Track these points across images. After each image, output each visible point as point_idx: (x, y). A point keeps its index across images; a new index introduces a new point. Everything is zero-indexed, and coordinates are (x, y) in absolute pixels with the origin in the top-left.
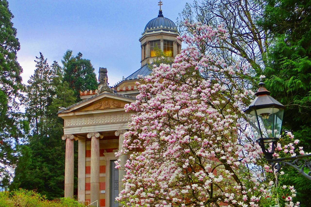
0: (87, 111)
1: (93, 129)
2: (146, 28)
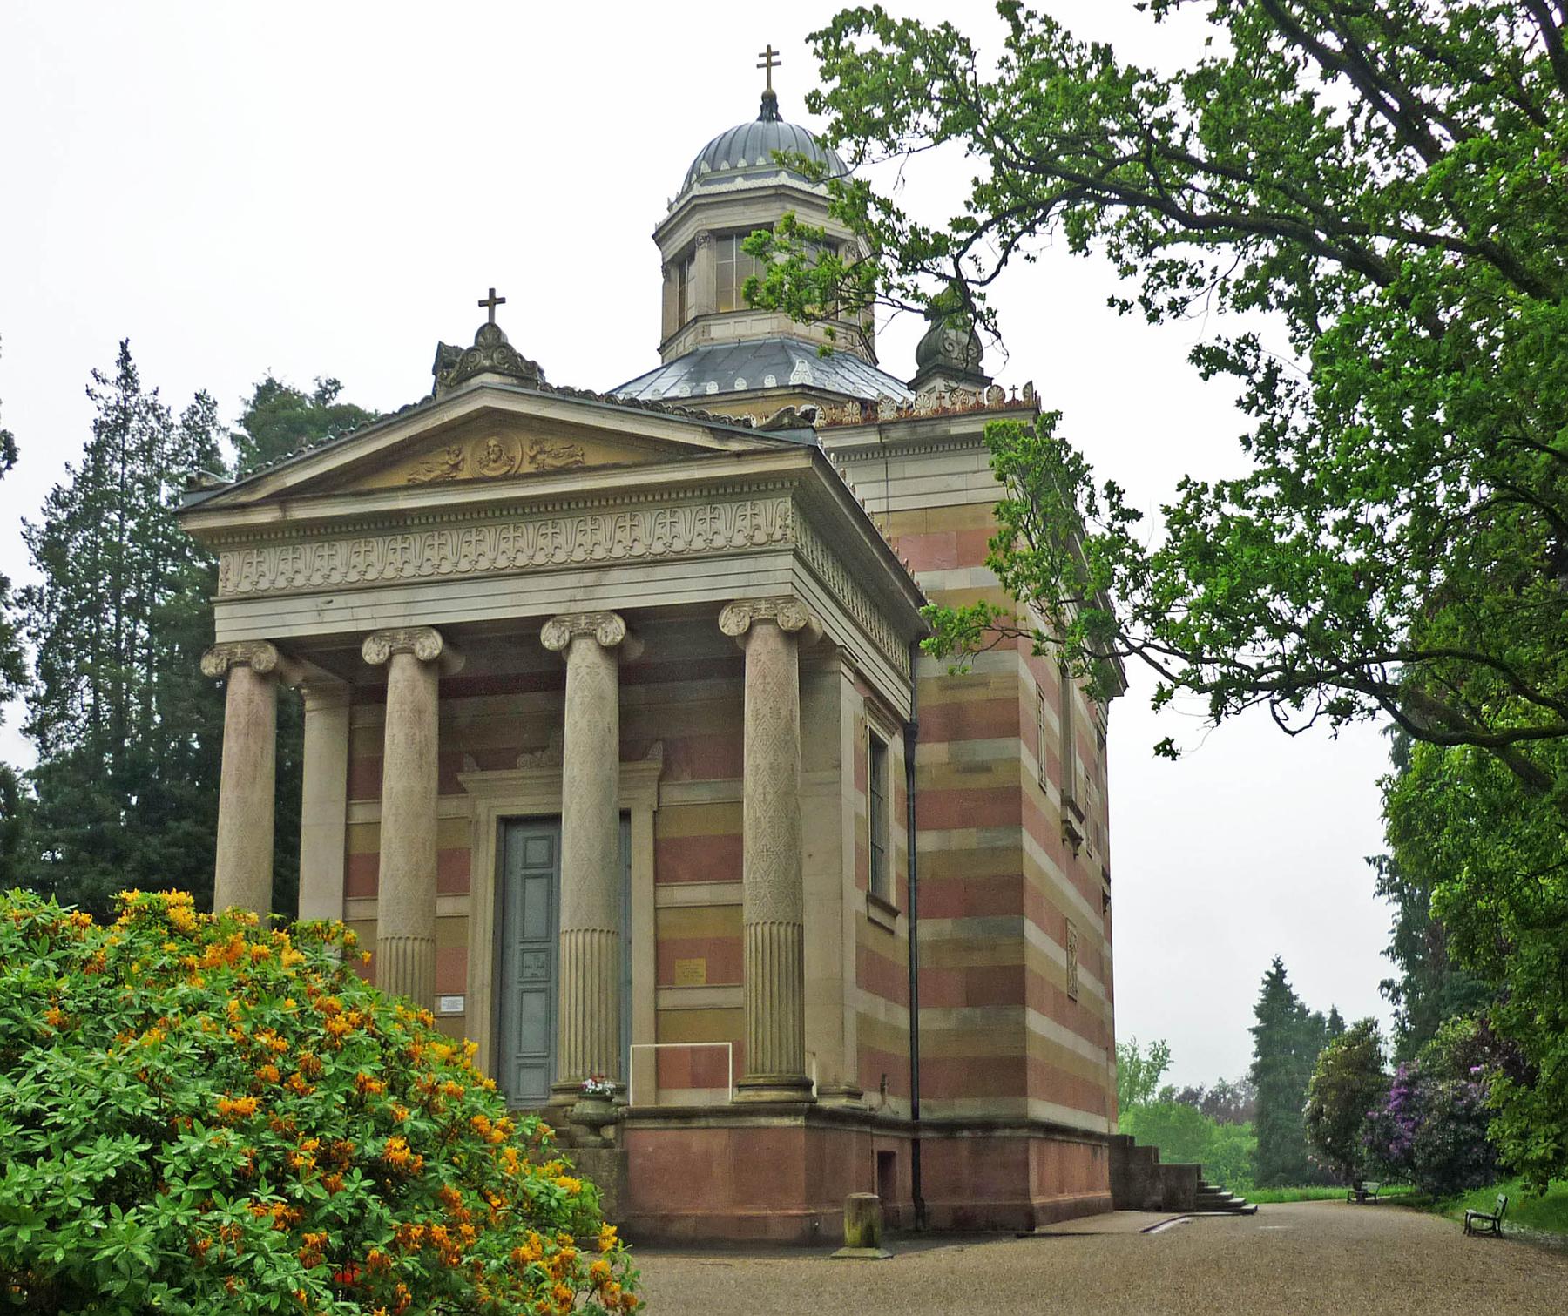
0: (371, 493)
2: (695, 168)
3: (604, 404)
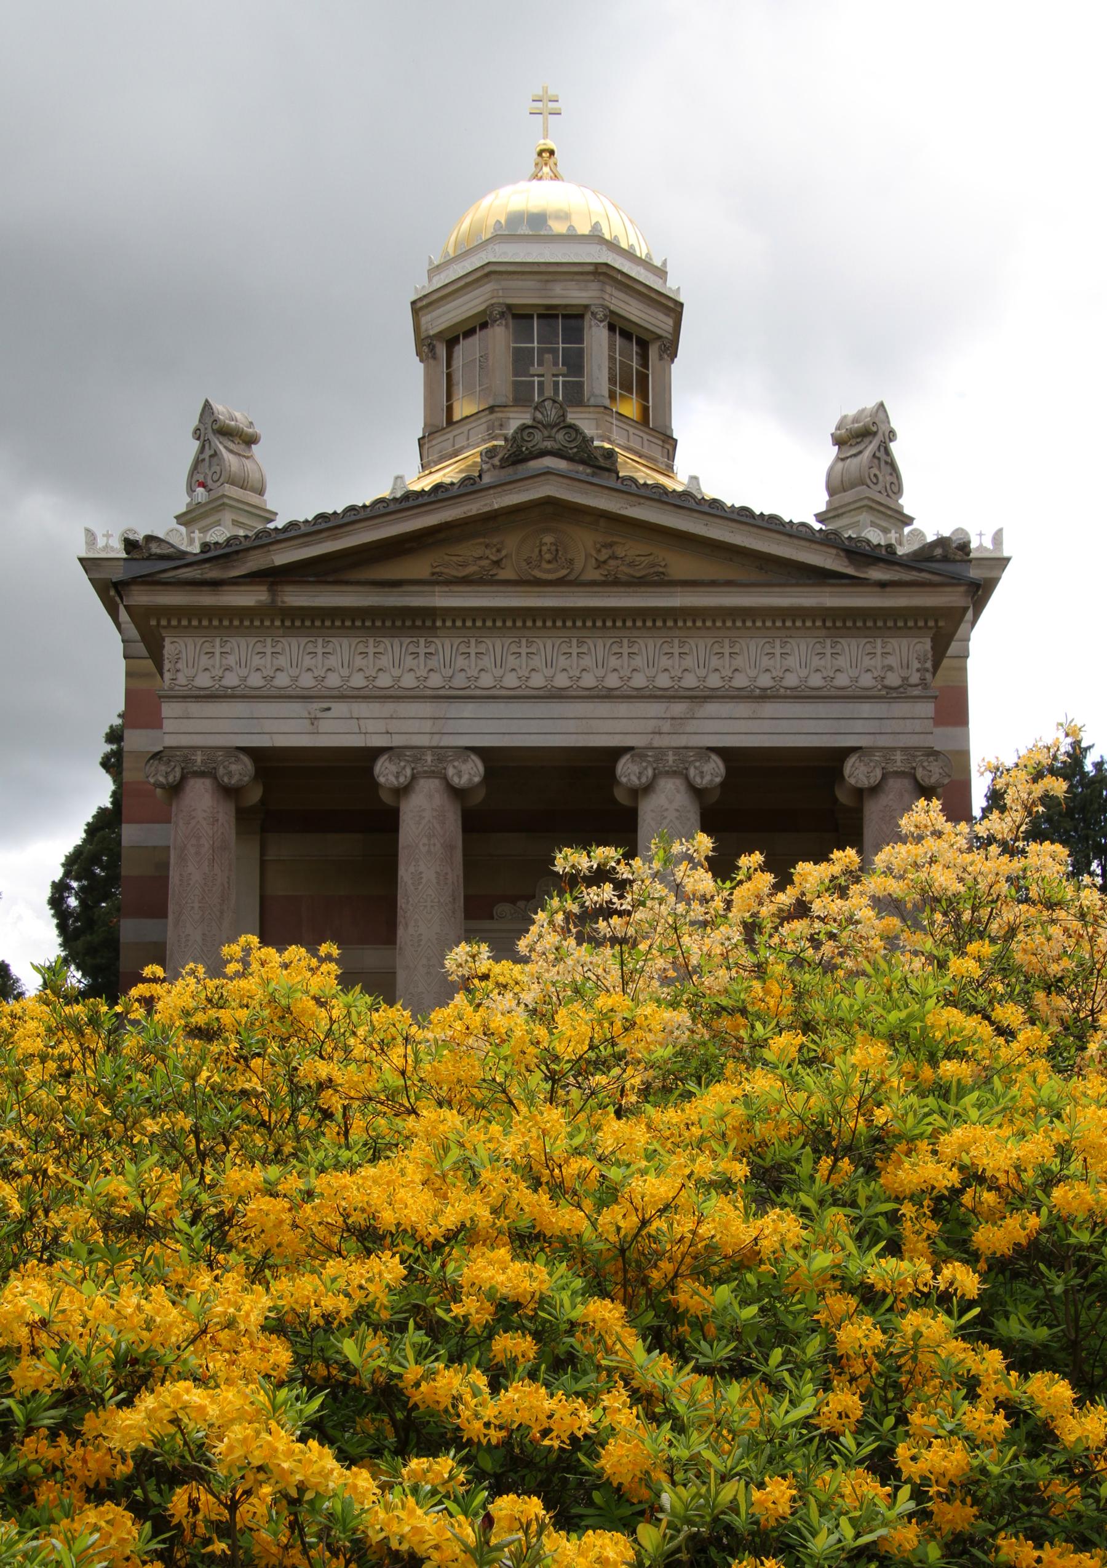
1: (427, 726)
3: (706, 509)
